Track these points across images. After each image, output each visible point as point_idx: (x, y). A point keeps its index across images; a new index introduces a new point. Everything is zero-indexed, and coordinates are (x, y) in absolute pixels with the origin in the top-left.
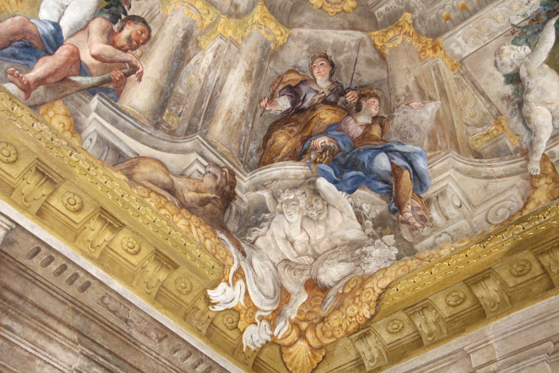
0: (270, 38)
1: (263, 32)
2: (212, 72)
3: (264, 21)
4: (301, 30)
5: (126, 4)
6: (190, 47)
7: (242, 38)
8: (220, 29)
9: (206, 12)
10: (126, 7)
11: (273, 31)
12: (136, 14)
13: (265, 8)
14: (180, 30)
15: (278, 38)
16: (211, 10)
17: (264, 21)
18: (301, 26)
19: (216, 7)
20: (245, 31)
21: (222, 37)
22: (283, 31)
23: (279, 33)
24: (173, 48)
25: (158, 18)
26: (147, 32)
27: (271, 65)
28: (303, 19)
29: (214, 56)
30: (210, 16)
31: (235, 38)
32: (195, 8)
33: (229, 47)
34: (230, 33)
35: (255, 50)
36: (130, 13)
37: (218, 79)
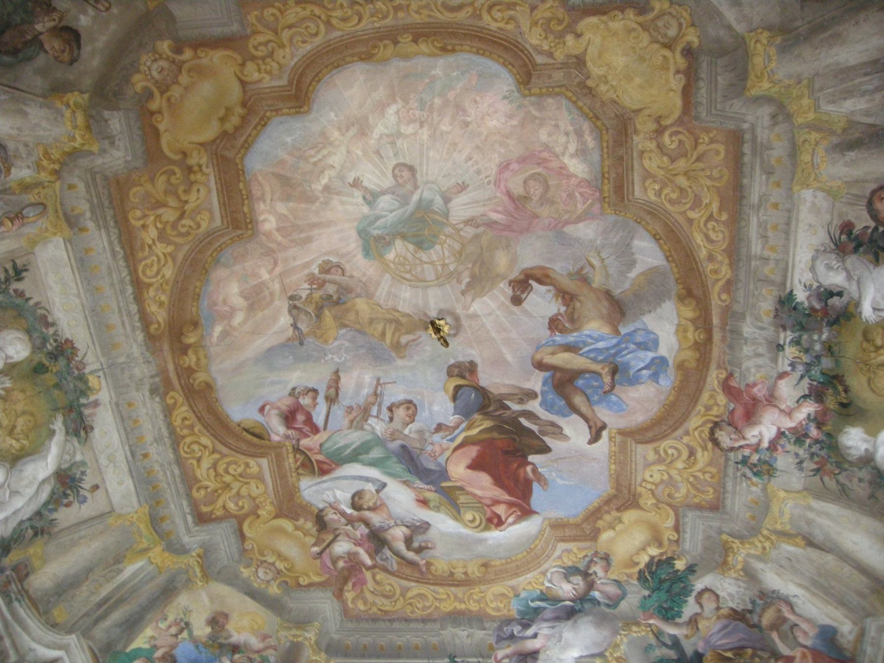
0: (773, 51)
1: (773, 65)
2: (864, 88)
3: (762, 73)
4: (734, 24)
5: (865, 234)
6: (857, 135)
7: (799, 82)
8: (811, 116)
9: (807, 145)
10: (870, 231)
11: (762, 53)
12: (868, 217)
13: (749, 84)
14: (847, 158)
15: (765, 42)
16: (801, 140)
17: (762, 73)
18: (729, 28)
19: (793, 137)
20: (789, 86)
21: (817, 107)
22: (752, 43)
23: (759, 45)
24: (873, 154)
25: (854, 191)
26: (878, 194)
27: (799, 23)
28: (722, 33)
29: (845, 99)
30: (807, 136)
31: (806, 92)
32: (812, 160)
33: (821, 89)
34: (806, 101)
35: (799, 56)
36: (872, 224)
37: (866, 74)
